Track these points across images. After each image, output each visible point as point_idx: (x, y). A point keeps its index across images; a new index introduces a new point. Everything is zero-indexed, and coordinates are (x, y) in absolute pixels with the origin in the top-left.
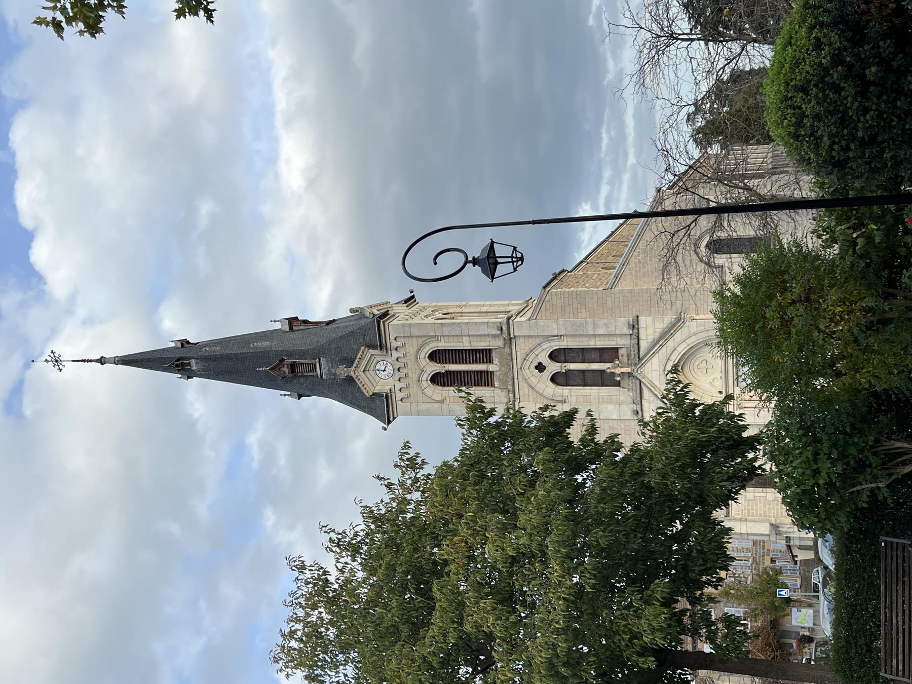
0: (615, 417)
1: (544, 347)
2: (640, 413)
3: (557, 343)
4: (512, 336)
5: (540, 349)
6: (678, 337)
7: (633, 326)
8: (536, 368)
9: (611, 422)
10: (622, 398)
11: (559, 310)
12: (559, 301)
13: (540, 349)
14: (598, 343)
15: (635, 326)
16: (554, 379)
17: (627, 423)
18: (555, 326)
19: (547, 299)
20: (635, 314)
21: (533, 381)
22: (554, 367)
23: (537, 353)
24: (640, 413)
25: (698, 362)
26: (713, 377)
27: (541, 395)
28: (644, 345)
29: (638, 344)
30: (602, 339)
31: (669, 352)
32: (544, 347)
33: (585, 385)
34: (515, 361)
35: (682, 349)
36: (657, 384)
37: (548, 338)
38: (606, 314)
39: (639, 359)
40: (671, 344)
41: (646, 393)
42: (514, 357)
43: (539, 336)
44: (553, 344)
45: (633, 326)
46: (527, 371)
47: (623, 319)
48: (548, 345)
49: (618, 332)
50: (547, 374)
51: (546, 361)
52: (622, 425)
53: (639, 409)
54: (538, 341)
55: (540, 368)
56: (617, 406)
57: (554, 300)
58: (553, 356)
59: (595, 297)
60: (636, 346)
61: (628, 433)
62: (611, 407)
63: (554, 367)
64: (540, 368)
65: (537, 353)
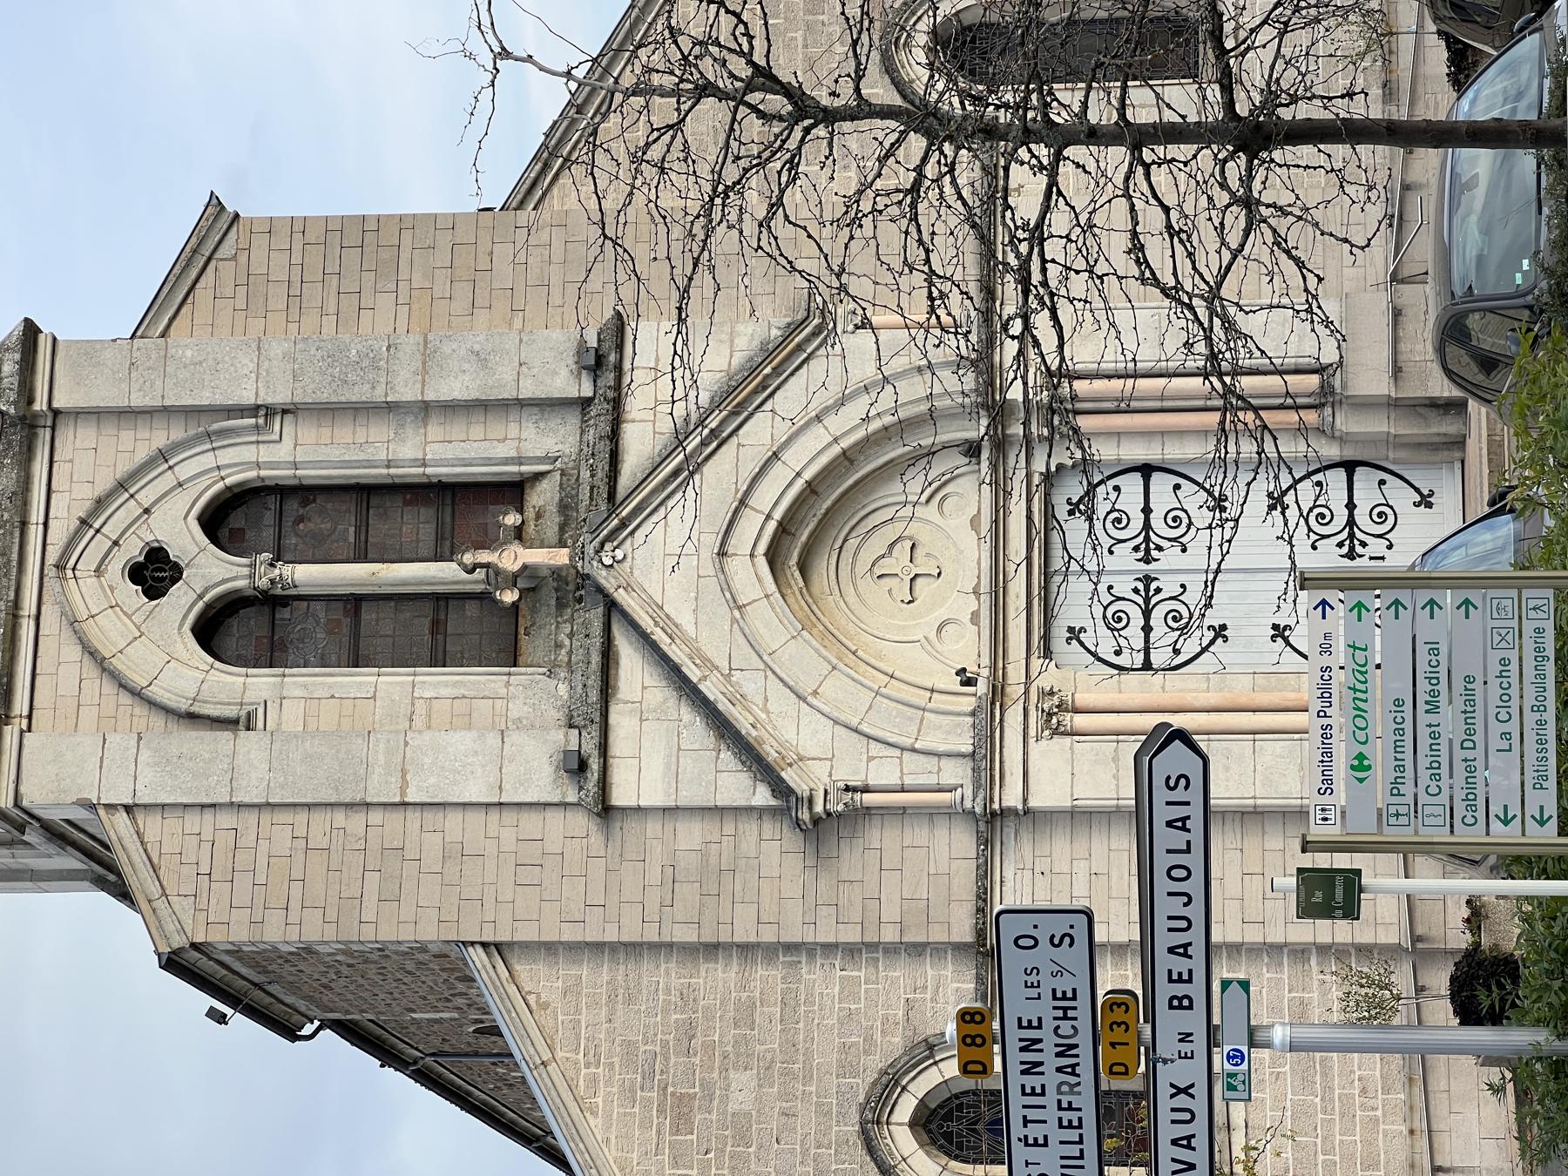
0: (475, 791)
1: (184, 471)
2: (594, 764)
3: (248, 453)
4: (40, 405)
5: (168, 480)
6: (792, 398)
7: (600, 360)
8: (136, 574)
9: (454, 819)
10: (517, 709)
11: (278, 301)
12: (280, 259)
13: (168, 480)
14: (433, 452)
15: (604, 359)
16: (214, 628)
17: (531, 823)
18: (247, 362)
19: (226, 250)
20: (609, 314)
21: (110, 632)
22: (212, 571)
23: (146, 497)
24: (594, 764)
25: (877, 545)
26: (941, 614)
27: (137, 694)
28: (642, 440)
29: (614, 436)
30: (457, 429)
31: (750, 468)
32: (184, 471)
33: (356, 659)
34: (35, 533)
35: (809, 455)
36: (685, 620)
37: (211, 421)
38: (482, 316)
39: (607, 500)
40: (759, 432)
41: (632, 668)
42: (36, 515)
43: (167, 412)
44: (226, 456)
45: (600, 360)
46: (89, 583)
47: (556, 335)
48: (208, 461)
49: (528, 390)
50: (182, 602)
51: (180, 534)
52: (508, 836)
53: (590, 747)
54: (160, 437)
55: (154, 573)
56: (493, 740)
57: (259, 255)
58: (224, 518)
59: (444, 240)
60: (604, 448)
61: (526, 875)
62: (461, 742)
63: (212, 571)
64: (154, 573)
65: (146, 497)
